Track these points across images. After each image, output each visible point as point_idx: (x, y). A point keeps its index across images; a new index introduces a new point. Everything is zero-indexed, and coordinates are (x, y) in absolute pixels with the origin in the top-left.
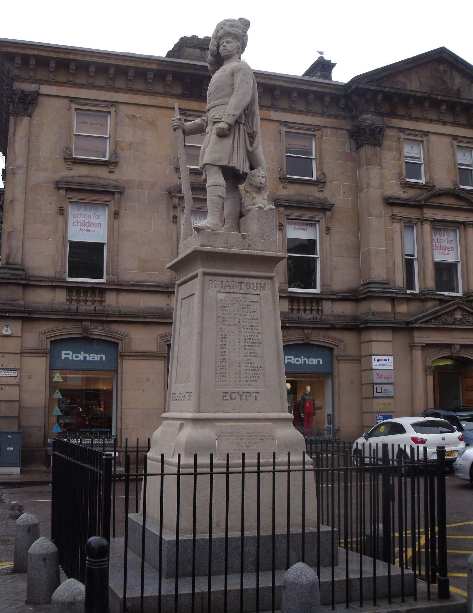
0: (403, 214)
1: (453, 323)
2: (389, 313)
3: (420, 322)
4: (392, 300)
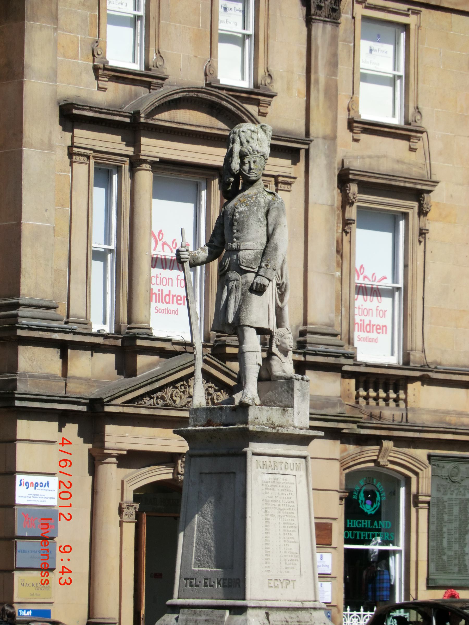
0: (94, 143)
1: (185, 406)
2: (55, 376)
3: (119, 401)
4: (63, 348)
